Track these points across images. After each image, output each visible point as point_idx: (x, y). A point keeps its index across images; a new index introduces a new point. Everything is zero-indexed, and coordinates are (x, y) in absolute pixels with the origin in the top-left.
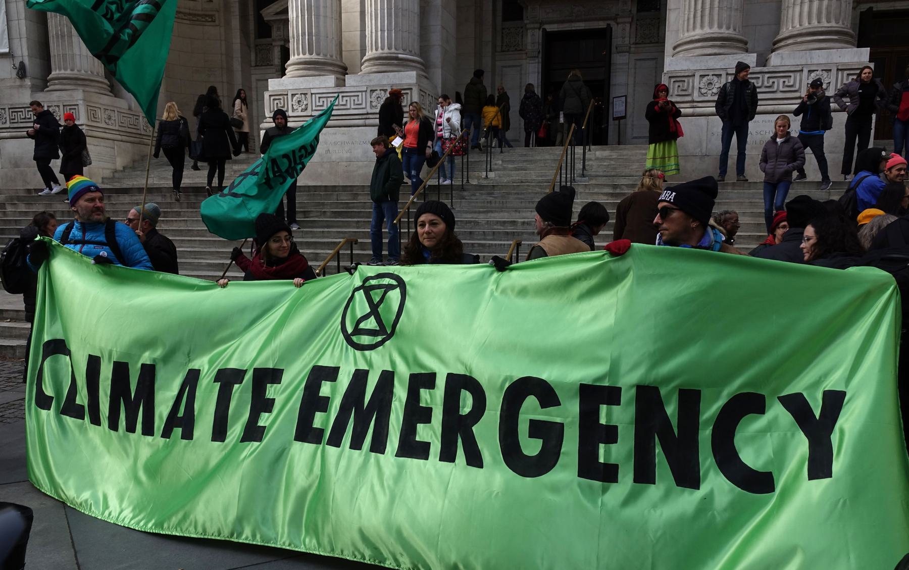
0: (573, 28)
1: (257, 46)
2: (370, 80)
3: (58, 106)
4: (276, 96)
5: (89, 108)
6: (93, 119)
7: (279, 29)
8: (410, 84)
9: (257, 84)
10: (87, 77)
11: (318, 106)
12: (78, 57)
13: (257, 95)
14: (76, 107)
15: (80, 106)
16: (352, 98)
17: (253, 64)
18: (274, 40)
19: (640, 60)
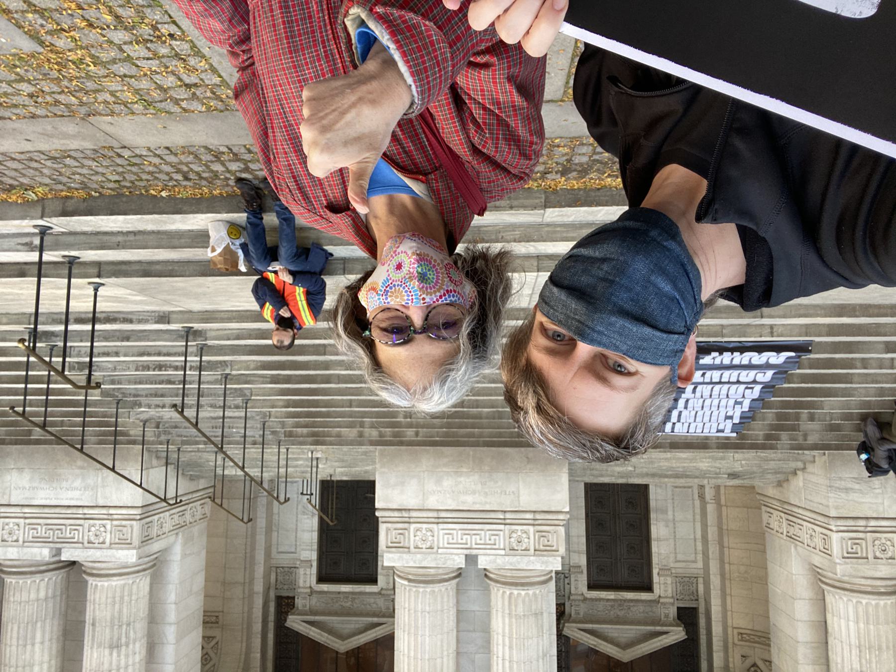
0: (351, 586)
1: (697, 600)
2: (436, 559)
3: (876, 558)
4: (549, 550)
5: (829, 552)
6: (826, 537)
7: (667, 616)
8: (389, 552)
9: (696, 558)
10: (839, 591)
11: (497, 535)
12: (851, 618)
13: (695, 545)
14: (846, 555)
15: (840, 555)
16: (454, 541)
17: (701, 580)
18: (673, 604)
19: (292, 553)
